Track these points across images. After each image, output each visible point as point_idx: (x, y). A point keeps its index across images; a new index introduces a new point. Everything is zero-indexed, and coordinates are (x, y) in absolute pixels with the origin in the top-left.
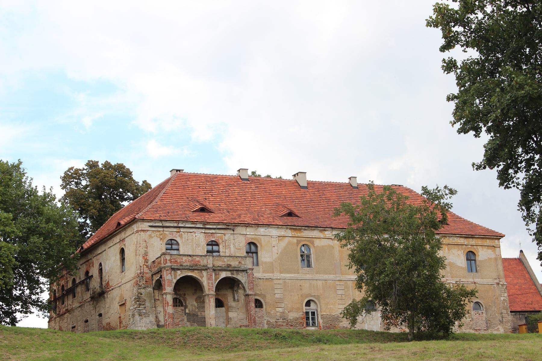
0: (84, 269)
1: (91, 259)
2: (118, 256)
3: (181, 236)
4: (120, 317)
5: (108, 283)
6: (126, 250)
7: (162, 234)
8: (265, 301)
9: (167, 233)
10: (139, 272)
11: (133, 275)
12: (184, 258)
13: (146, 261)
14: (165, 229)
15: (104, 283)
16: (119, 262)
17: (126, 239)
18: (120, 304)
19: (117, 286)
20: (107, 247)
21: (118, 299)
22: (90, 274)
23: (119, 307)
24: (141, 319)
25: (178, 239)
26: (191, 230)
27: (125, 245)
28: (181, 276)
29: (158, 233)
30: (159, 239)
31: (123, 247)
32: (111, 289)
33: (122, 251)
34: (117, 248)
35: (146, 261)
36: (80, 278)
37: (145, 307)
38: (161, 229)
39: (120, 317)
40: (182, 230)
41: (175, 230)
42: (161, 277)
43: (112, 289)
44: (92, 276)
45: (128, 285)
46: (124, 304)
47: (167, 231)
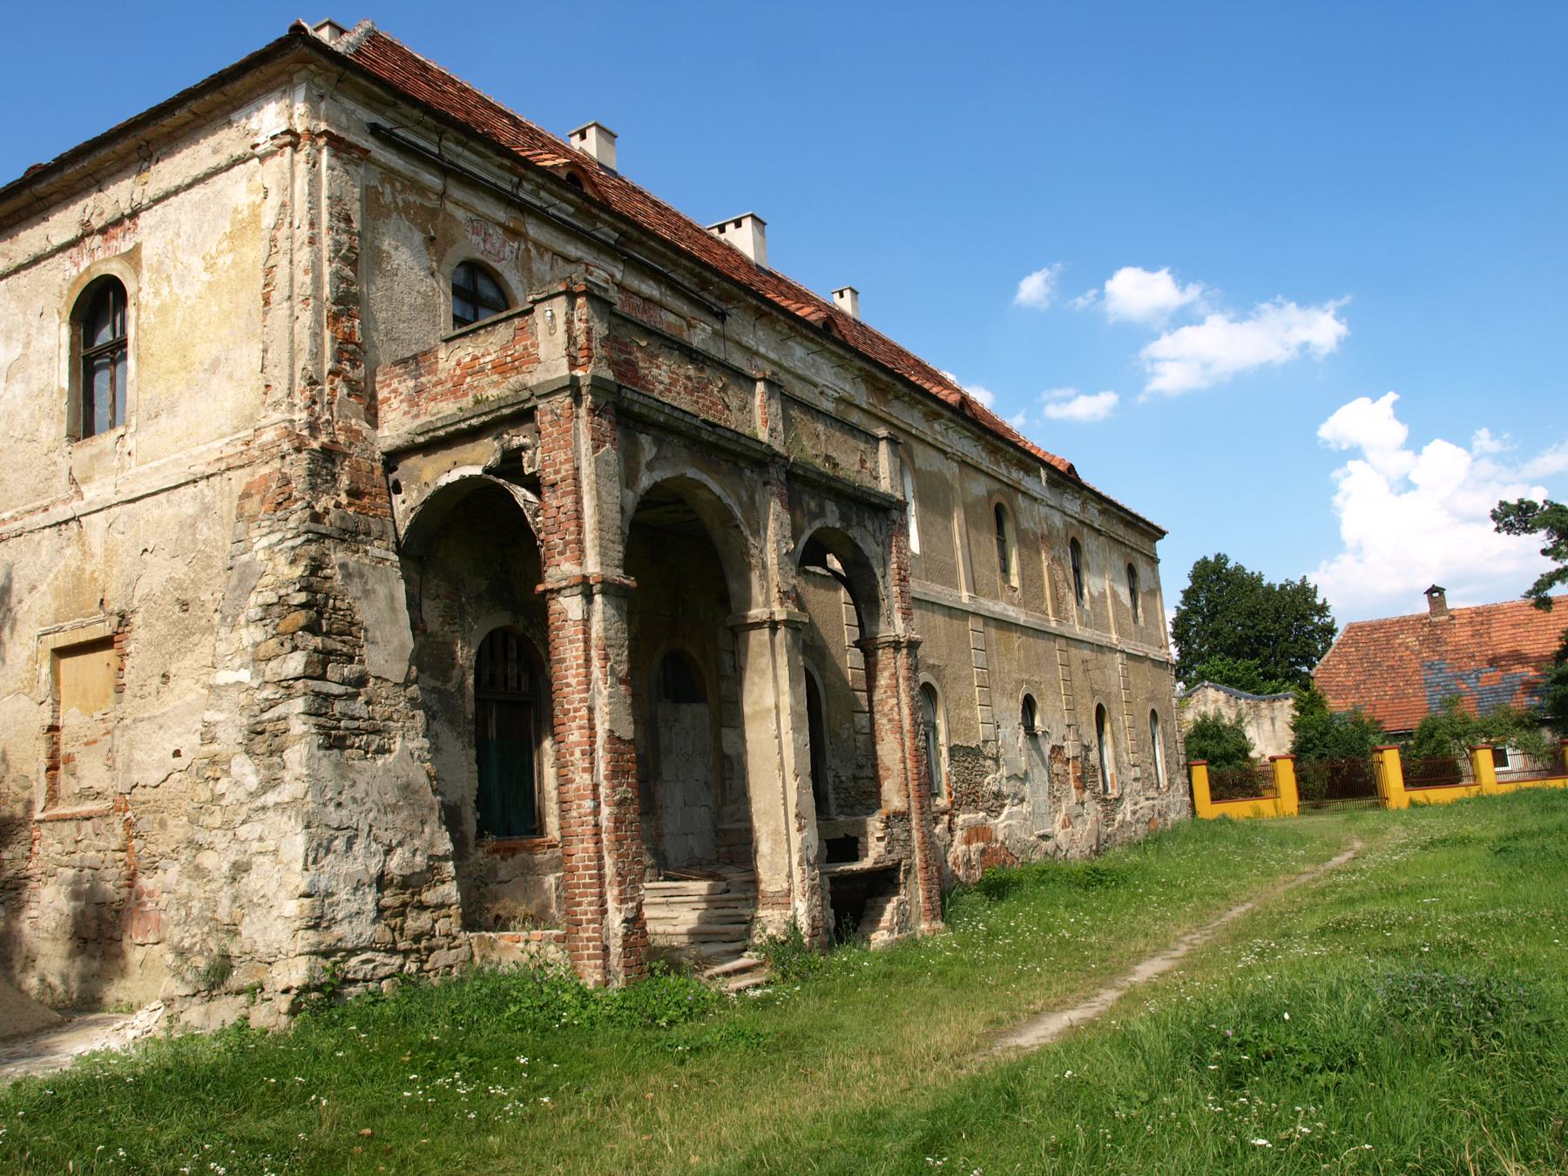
2: (57, 336)
3: (524, 265)
4: (54, 729)
6: (144, 295)
7: (433, 213)
8: (823, 677)
9: (460, 214)
14: (457, 193)
16: (60, 375)
17: (145, 219)
18: (62, 640)
19: (40, 519)
26: (573, 250)
27: (132, 257)
28: (658, 476)
30: (418, 237)
31: (116, 269)
33: (100, 304)
34: (64, 279)
37: (361, 681)
38: (431, 179)
39: (54, 729)
40: (533, 230)
41: (500, 214)
42: (510, 463)
46: (104, 643)
47: (463, 207)
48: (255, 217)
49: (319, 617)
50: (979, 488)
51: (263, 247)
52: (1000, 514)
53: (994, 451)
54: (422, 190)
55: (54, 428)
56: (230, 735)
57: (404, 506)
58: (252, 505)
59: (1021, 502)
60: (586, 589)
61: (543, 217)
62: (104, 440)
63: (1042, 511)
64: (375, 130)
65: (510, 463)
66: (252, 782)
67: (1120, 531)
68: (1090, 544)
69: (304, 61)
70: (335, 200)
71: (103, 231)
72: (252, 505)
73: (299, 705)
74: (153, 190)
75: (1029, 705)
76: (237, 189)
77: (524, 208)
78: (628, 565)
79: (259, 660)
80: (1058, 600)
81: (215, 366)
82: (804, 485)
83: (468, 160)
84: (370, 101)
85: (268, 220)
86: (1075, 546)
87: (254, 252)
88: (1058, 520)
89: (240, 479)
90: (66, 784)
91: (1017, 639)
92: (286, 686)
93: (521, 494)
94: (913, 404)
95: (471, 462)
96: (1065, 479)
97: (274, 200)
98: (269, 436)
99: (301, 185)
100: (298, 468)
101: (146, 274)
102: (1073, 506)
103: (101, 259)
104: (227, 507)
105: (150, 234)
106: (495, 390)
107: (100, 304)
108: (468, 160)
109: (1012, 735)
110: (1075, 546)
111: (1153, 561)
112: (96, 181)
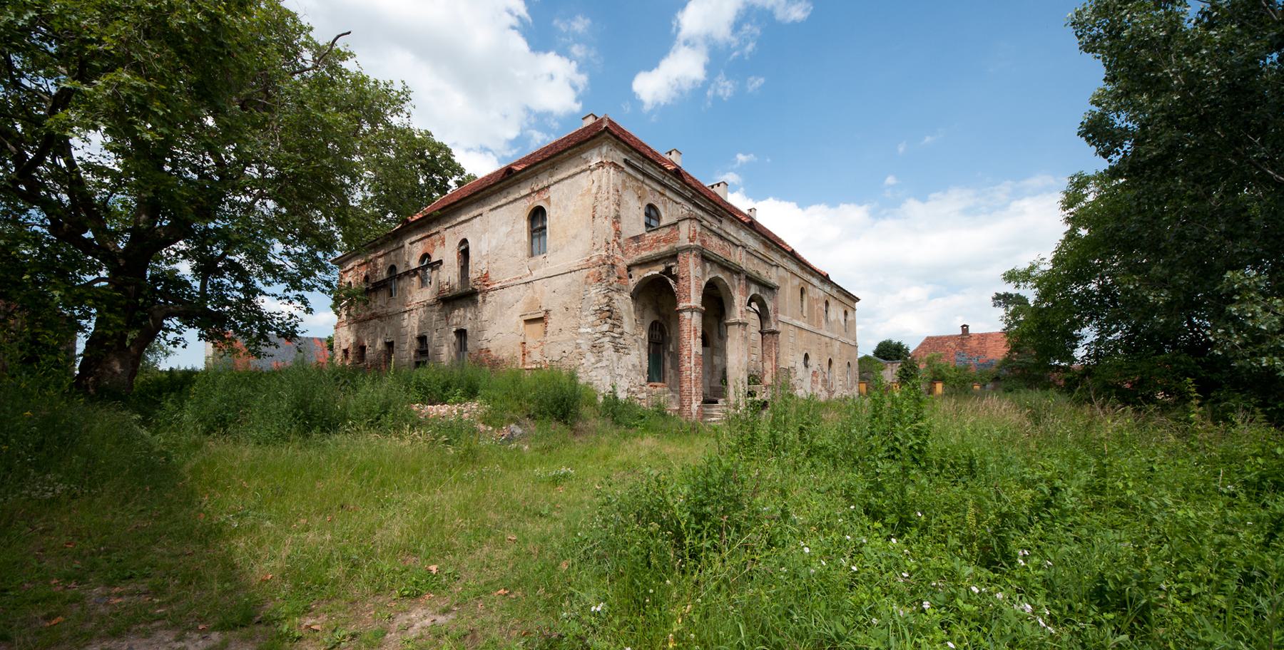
0: (419, 249)
1: (438, 233)
2: (524, 224)
5: (486, 277)
6: (552, 213)
10: (604, 253)
11: (574, 262)
12: (715, 240)
13: (618, 233)
14: (647, 181)
15: (473, 275)
16: (524, 236)
19: (519, 281)
20: (487, 208)
21: (520, 308)
22: (435, 259)
23: (522, 324)
24: (619, 359)
25: (661, 208)
26: (679, 200)
27: (548, 200)
29: (634, 183)
32: (497, 286)
33: (537, 215)
34: (524, 208)
35: (618, 233)
36: (407, 264)
37: (622, 334)
40: (668, 193)
41: (659, 188)
42: (668, 271)
43: (502, 288)
44: (440, 262)
45: (559, 282)
46: (541, 319)
48: (590, 190)
49: (609, 314)
50: (797, 281)
51: (592, 199)
52: (802, 291)
53: (803, 269)
54: (637, 180)
55: (522, 252)
56: (585, 346)
57: (632, 283)
58: (590, 280)
59: (810, 287)
60: (691, 310)
61: (671, 189)
62: (540, 258)
63: (817, 291)
64: (625, 161)
65: (668, 271)
66: (593, 360)
67: (843, 299)
68: (832, 302)
69: (607, 138)
70: (615, 185)
71: (538, 192)
72: (590, 280)
73: (608, 339)
74: (555, 179)
75: (806, 357)
76: (584, 181)
77: (665, 186)
78: (703, 304)
79: (593, 326)
80: (820, 321)
81: (575, 237)
82: (751, 279)
83: (650, 170)
84: (624, 151)
85: (594, 191)
86: (827, 303)
87: (589, 201)
88: (822, 294)
89: (585, 272)
90: (528, 360)
91: (805, 334)
92: (604, 334)
93: (671, 282)
94: (777, 252)
95: (656, 270)
96: (825, 279)
97: (596, 184)
98: (595, 259)
99: (604, 180)
100: (604, 270)
101: (552, 206)
102: (827, 289)
103: (537, 201)
104: (582, 280)
105: (554, 193)
106: (664, 248)
107: (537, 215)
108: (650, 170)
109: (800, 365)
110: (827, 303)
111: (854, 309)
112: (535, 174)
